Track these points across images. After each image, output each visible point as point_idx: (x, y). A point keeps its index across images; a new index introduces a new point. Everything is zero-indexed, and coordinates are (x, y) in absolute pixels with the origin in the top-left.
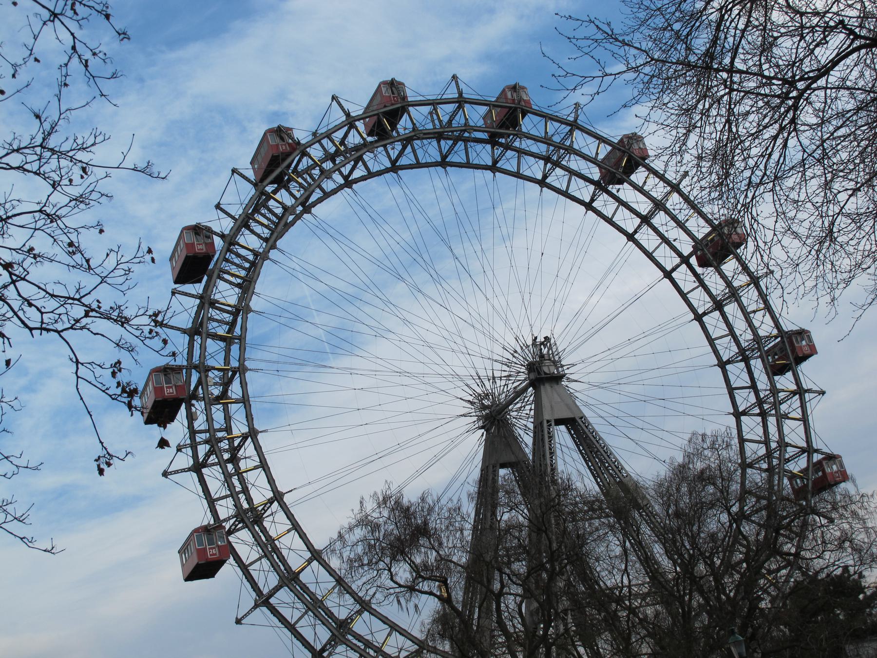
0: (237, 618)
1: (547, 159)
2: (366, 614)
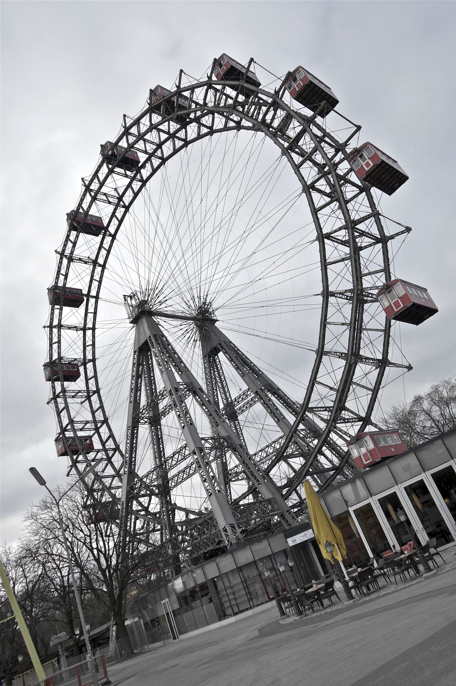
0: (408, 371)
1: (88, 398)
2: (331, 289)
